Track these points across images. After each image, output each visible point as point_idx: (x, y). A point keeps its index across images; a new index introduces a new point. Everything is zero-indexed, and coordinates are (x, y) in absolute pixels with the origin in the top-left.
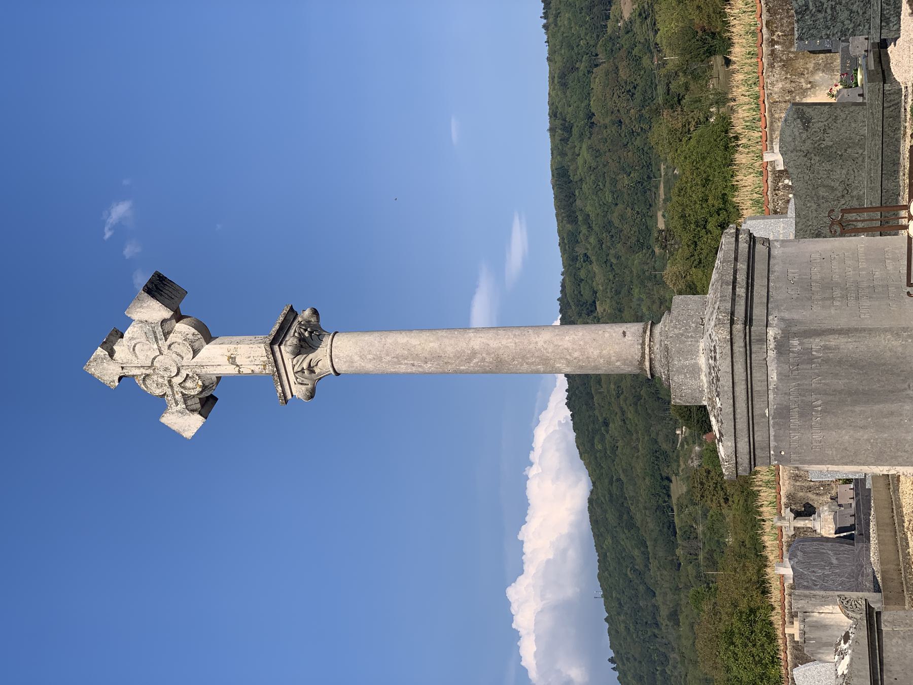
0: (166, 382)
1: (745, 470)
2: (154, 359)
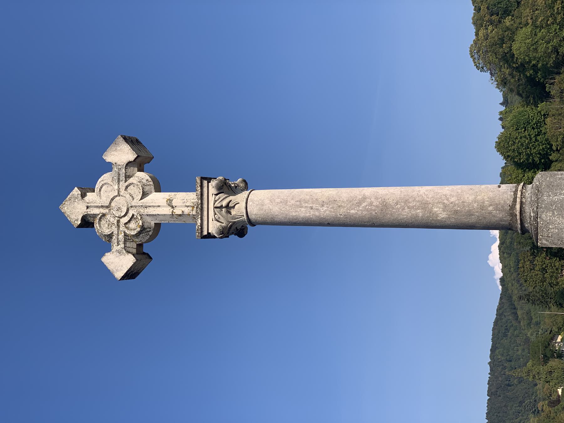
0: (115, 222)
2: (112, 199)
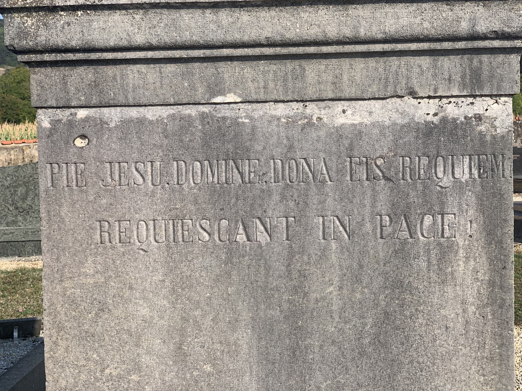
1: (23, 33)
